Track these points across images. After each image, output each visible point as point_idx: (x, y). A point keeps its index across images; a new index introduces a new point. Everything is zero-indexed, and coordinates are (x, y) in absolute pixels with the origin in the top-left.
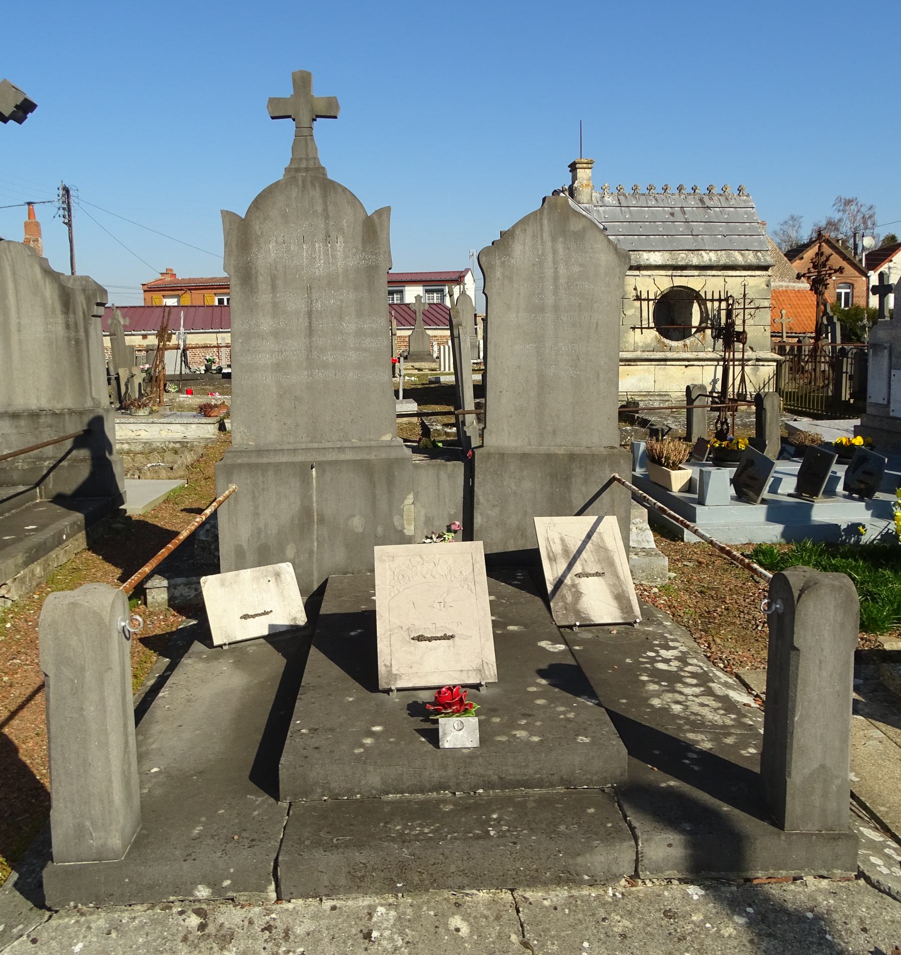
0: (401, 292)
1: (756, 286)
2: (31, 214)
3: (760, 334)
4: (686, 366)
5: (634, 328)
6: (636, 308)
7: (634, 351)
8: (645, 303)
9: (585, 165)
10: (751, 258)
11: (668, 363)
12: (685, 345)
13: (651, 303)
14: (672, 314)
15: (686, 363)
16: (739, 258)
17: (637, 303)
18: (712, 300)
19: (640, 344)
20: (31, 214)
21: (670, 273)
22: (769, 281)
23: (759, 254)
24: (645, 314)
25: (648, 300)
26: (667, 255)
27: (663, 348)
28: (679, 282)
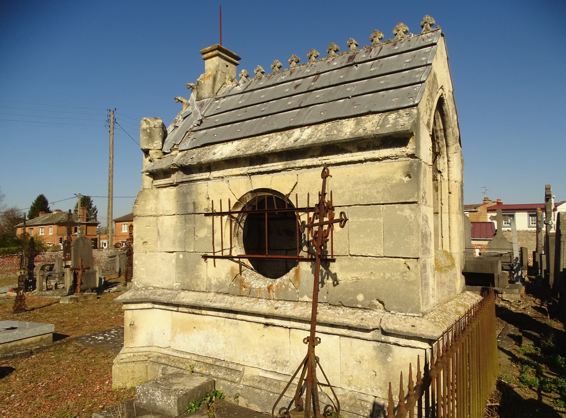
0: (513, 216)
1: (384, 179)
3: (398, 276)
4: (267, 325)
5: (205, 257)
6: (208, 227)
7: (207, 291)
8: (217, 219)
9: (210, 54)
10: (371, 125)
11: (239, 316)
12: (269, 288)
13: (225, 217)
14: (274, 235)
15: (263, 320)
16: (348, 129)
17: (209, 220)
18: (307, 210)
19: (214, 282)
21: (245, 170)
22: (411, 165)
23: (393, 116)
24: (218, 236)
25: (222, 214)
26: (246, 142)
27: (239, 288)
28: (260, 182)
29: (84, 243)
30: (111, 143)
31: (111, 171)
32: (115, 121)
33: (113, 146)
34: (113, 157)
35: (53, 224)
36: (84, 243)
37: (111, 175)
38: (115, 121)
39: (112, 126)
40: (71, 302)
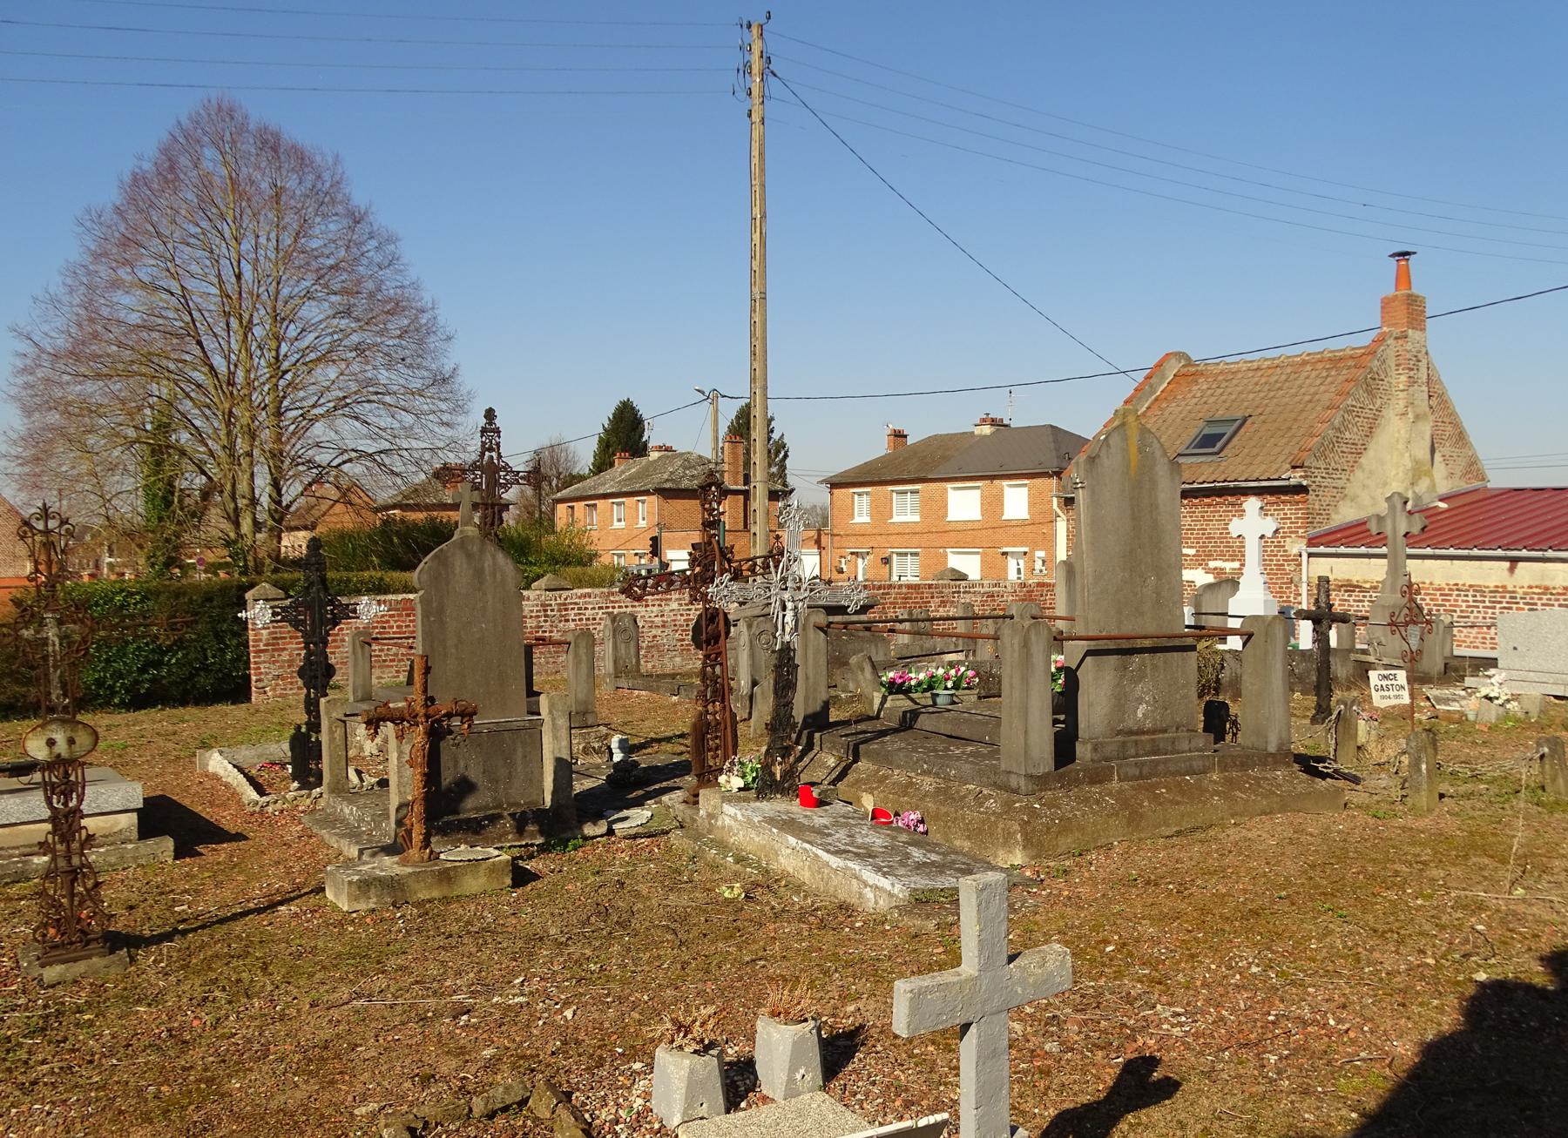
2: (1403, 278)
20: (1403, 278)
29: (479, 573)
30: (755, 161)
31: (758, 277)
32: (768, 71)
33: (762, 170)
34: (763, 216)
35: (646, 493)
36: (479, 573)
37: (756, 290)
38: (768, 71)
39: (755, 92)
40: (363, 906)
